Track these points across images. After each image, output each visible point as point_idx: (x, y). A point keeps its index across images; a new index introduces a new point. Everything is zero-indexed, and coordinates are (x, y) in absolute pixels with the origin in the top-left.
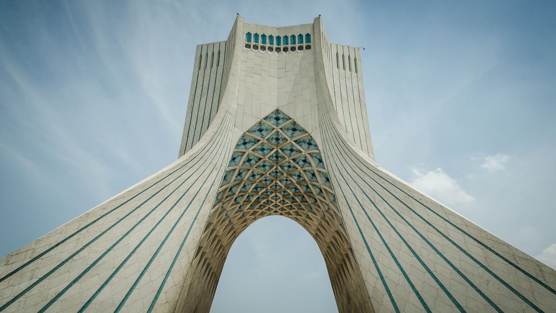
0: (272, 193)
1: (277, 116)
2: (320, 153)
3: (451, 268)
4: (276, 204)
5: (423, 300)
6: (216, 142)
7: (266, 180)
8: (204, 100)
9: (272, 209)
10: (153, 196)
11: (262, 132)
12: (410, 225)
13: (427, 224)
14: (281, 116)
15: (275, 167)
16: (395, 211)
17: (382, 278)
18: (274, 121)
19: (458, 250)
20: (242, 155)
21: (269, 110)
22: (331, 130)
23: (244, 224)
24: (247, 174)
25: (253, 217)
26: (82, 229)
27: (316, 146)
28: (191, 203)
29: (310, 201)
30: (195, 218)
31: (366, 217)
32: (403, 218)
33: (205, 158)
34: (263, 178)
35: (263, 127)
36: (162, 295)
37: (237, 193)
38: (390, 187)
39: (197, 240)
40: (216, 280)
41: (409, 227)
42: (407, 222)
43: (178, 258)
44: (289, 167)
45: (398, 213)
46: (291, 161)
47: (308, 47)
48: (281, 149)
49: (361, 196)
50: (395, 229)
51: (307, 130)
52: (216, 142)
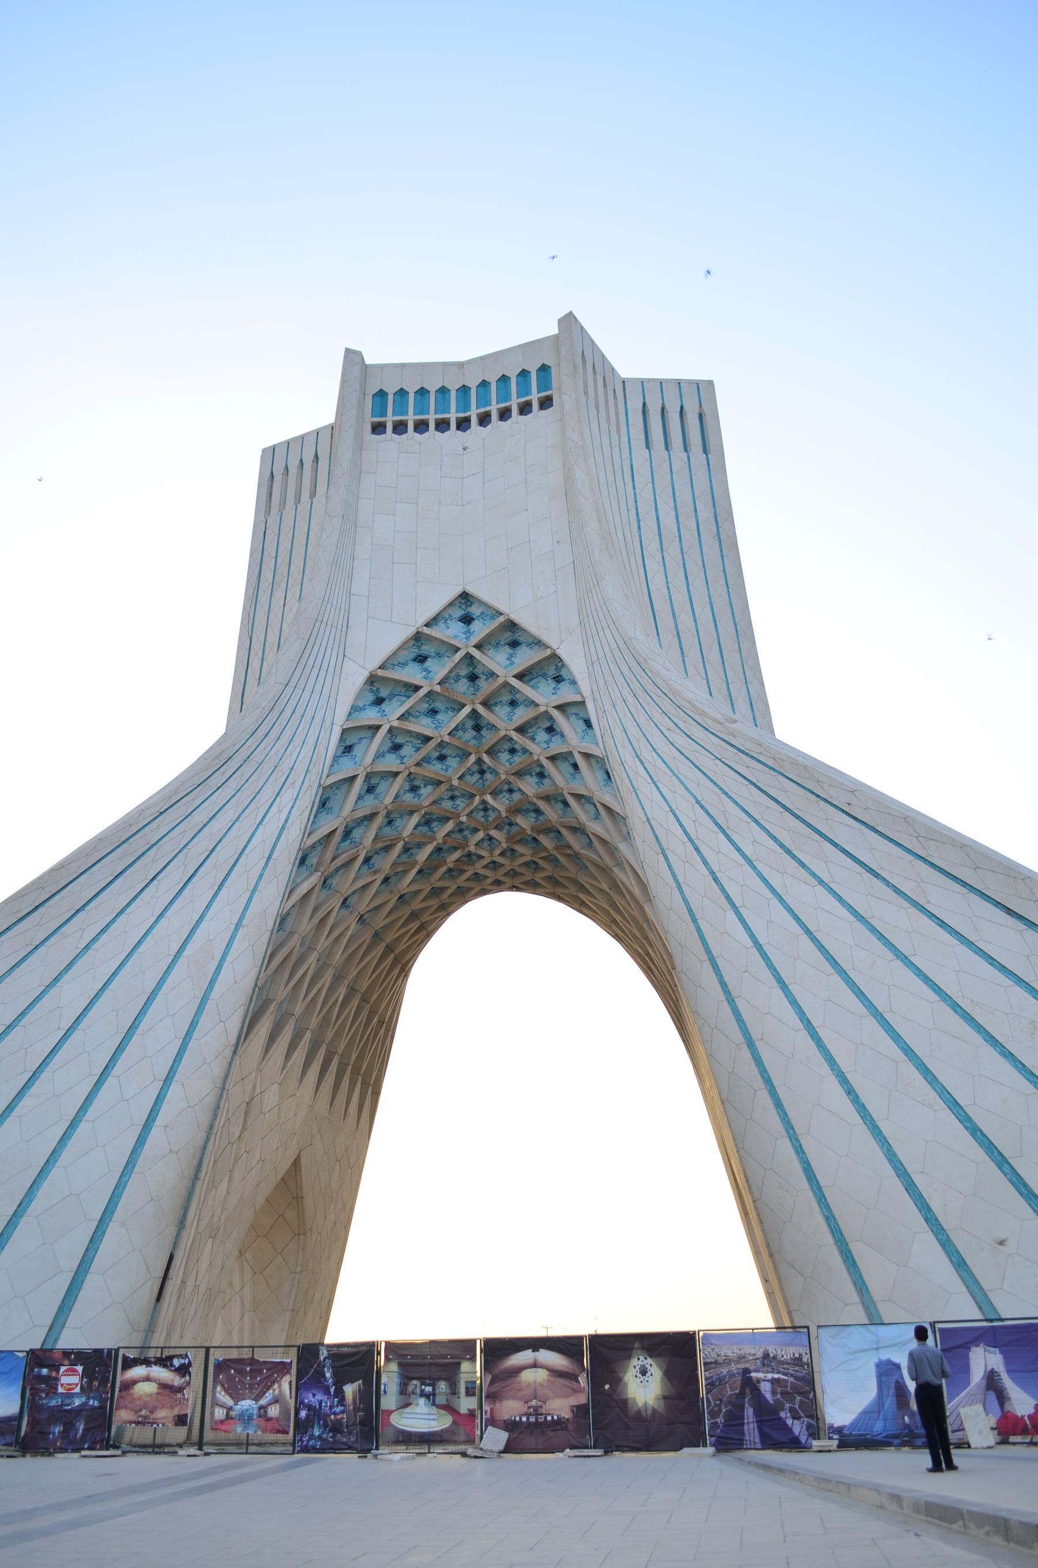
0: (476, 830)
2: (582, 703)
3: (934, 997)
4: (494, 862)
5: (858, 1097)
6: (289, 710)
7: (452, 798)
8: (279, 595)
9: (486, 877)
10: (117, 877)
11: (428, 664)
12: (821, 882)
13: (867, 876)
14: (475, 610)
15: (472, 759)
16: (782, 846)
17: (750, 1043)
19: (954, 941)
20: (374, 735)
22: (607, 631)
23: (414, 926)
25: (434, 903)
27: (574, 682)
28: (222, 885)
30: (238, 926)
31: (706, 872)
32: (802, 865)
33: (257, 757)
35: (427, 649)
37: (368, 841)
38: (766, 779)
39: (247, 983)
40: (365, 1083)
41: (820, 889)
42: (814, 875)
43: (195, 1035)
45: (789, 852)
46: (514, 735)
47: (546, 403)
48: (485, 704)
50: (781, 900)
51: (545, 638)
52: (289, 710)
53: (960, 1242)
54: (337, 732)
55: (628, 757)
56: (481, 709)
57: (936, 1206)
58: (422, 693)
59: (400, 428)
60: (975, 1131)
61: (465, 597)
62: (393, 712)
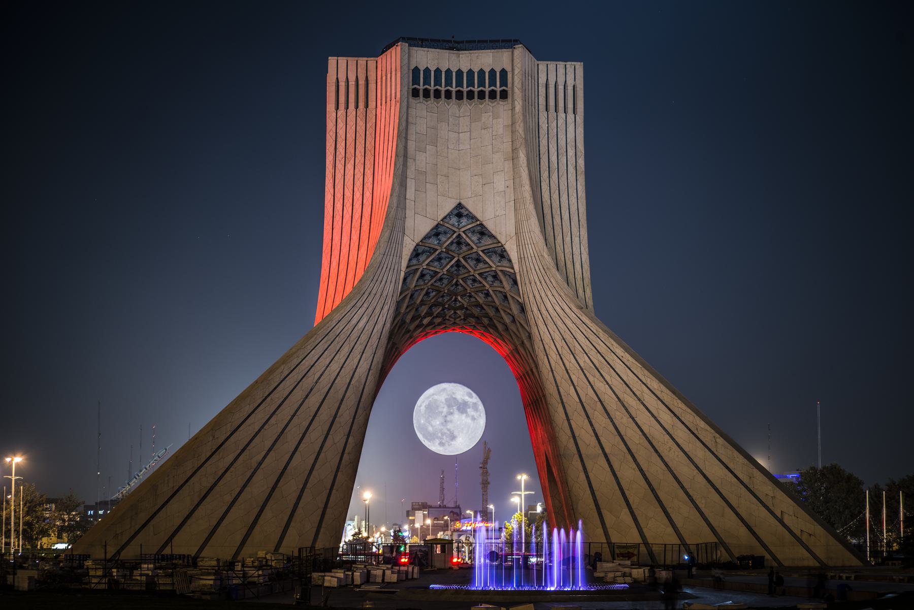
1: (460, 211)
8: (350, 166)
18: (454, 220)
21: (448, 206)
24: (419, 295)
26: (266, 398)
27: (510, 261)
29: (500, 327)
30: (370, 370)
33: (374, 292)
34: (441, 294)
36: (345, 455)
44: (474, 280)
47: (504, 95)
48: (463, 257)
49: (560, 343)
53: (636, 513)
54: (402, 274)
55: (535, 309)
56: (462, 260)
57: (631, 501)
58: (437, 253)
59: (427, 94)
60: (646, 479)
61: (460, 206)
62: (425, 262)
